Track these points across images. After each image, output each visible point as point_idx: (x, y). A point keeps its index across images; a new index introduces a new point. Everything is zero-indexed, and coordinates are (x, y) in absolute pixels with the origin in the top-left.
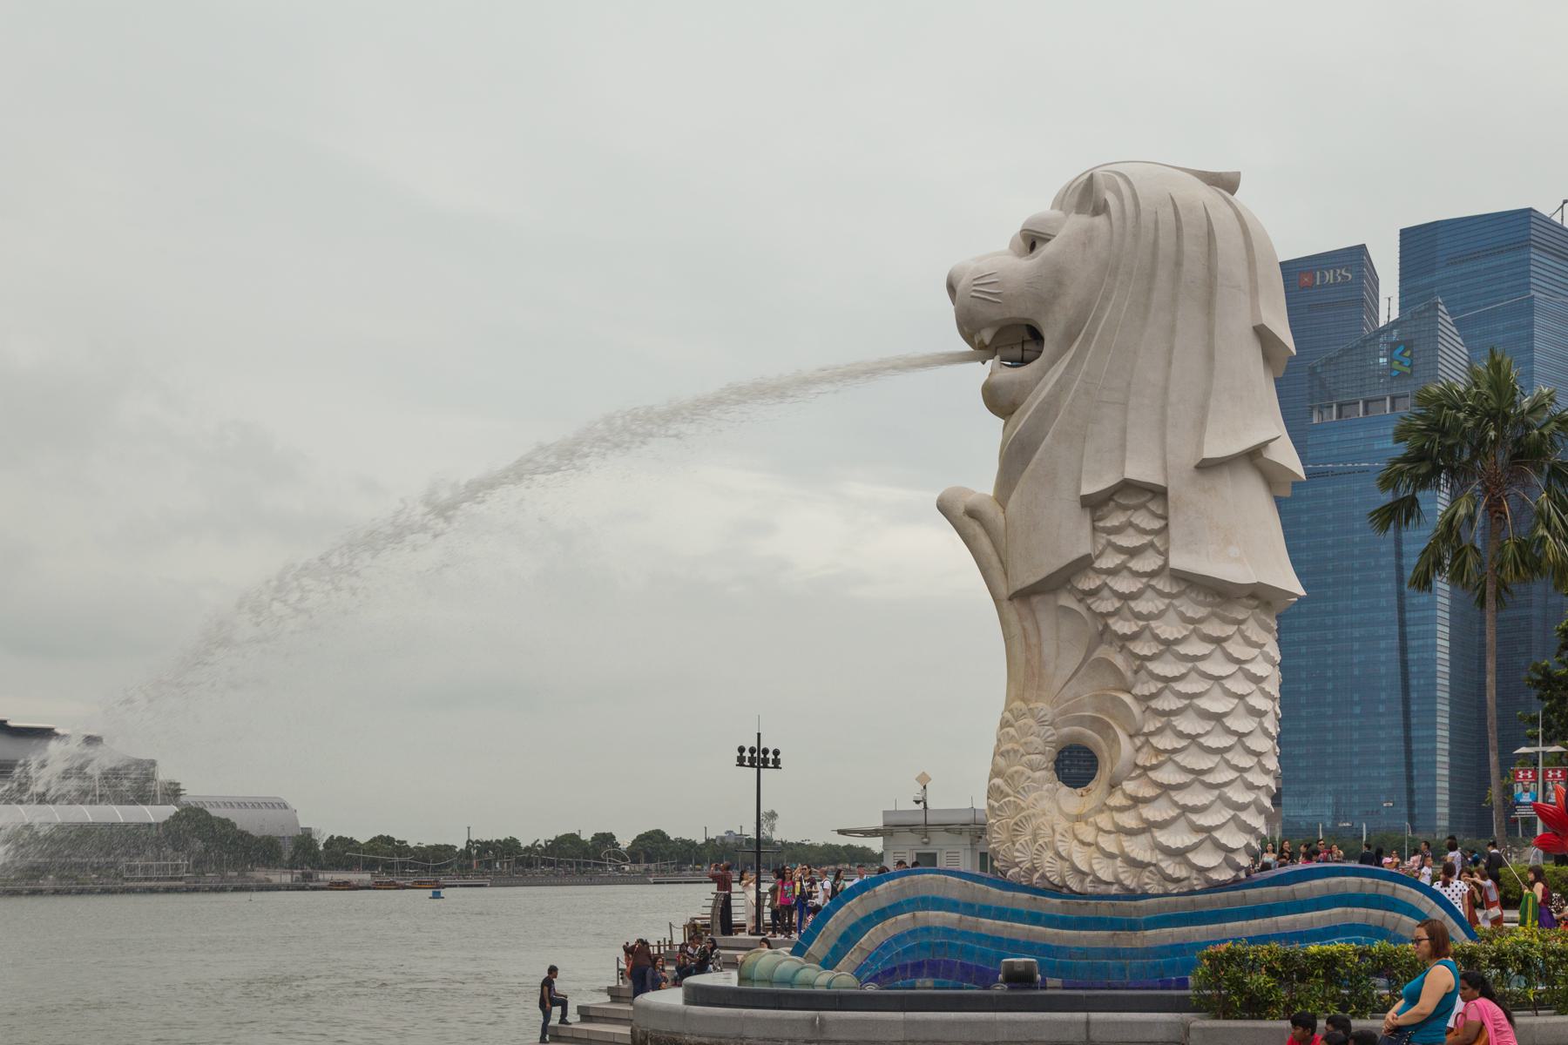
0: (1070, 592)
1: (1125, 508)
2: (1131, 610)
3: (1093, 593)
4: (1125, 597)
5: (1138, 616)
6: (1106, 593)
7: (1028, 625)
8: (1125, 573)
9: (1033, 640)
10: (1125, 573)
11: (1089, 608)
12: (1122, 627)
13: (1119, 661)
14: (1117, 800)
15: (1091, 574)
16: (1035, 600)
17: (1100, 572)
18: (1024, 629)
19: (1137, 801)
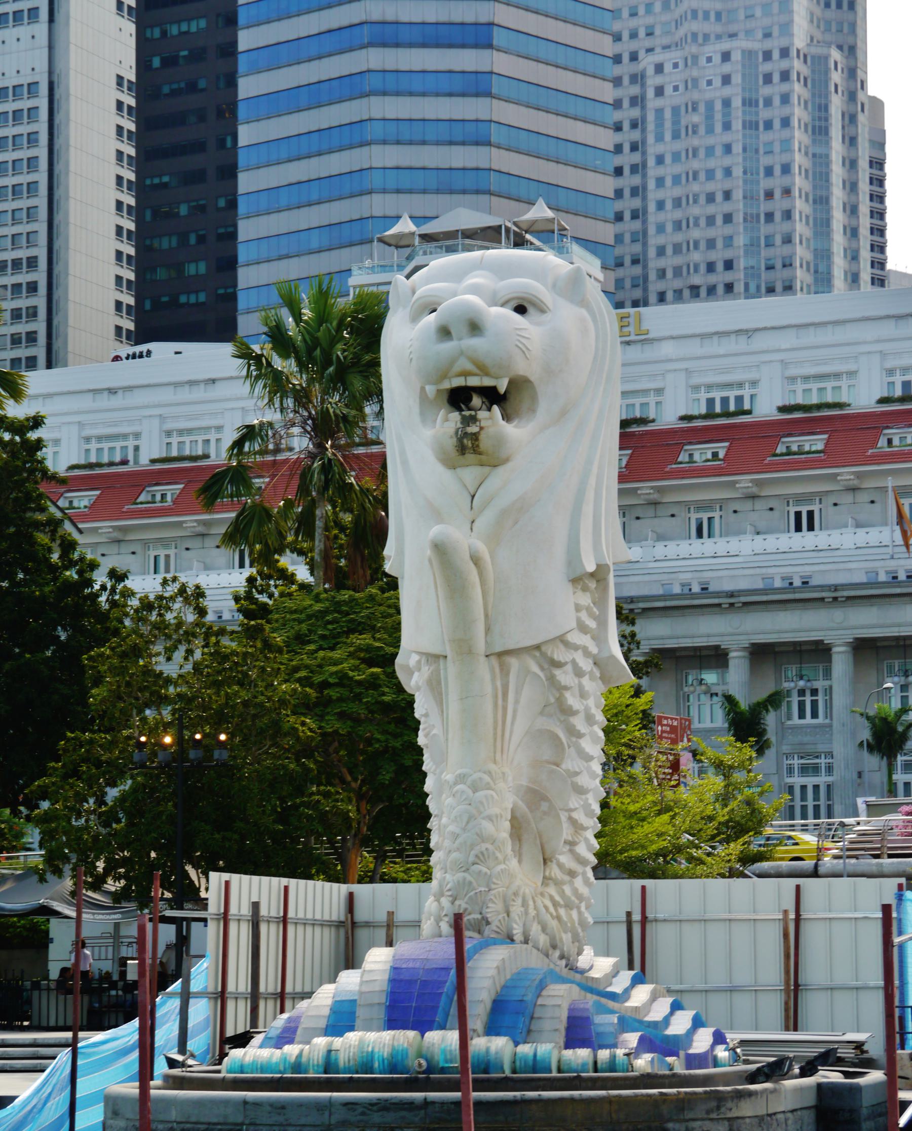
0: (534, 657)
1: (585, 589)
2: (581, 687)
3: (558, 665)
4: (579, 673)
5: (583, 695)
6: (569, 668)
7: (499, 684)
8: (580, 652)
9: (500, 702)
10: (580, 652)
11: (552, 679)
12: (572, 700)
13: (562, 735)
14: (555, 872)
15: (561, 646)
16: (513, 662)
17: (567, 644)
18: (495, 689)
19: (572, 874)
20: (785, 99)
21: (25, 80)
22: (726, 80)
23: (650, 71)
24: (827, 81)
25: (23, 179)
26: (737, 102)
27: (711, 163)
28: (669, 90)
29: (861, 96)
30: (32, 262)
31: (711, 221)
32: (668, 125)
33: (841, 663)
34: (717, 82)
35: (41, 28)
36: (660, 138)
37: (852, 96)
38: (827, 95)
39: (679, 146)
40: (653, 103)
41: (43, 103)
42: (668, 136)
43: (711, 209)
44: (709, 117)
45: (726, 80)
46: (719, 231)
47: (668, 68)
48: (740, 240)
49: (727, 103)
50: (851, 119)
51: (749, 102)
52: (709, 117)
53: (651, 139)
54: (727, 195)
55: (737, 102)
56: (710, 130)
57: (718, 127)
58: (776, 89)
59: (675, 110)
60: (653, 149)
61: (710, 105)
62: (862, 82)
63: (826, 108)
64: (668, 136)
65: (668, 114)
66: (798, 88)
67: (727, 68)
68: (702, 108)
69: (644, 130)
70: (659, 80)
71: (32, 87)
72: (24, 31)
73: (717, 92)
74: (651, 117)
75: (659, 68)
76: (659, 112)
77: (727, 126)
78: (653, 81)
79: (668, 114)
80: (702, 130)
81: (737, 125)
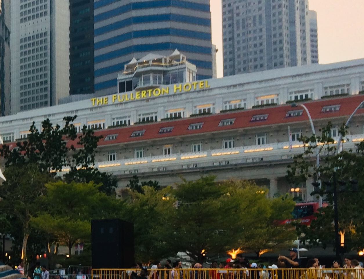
20: (280, 13)
21: (44, 31)
22: (260, 9)
23: (235, 8)
24: (294, 6)
25: (43, 59)
26: (264, 16)
27: (256, 35)
28: (241, 14)
29: (306, 10)
30: (46, 82)
31: (256, 53)
32: (241, 24)
33: (273, 185)
34: (257, 10)
35: (48, 17)
36: (238, 28)
37: (303, 10)
38: (294, 10)
39: (245, 31)
40: (236, 18)
41: (48, 37)
42: (241, 28)
43: (255, 49)
44: (255, 20)
45: (260, 9)
46: (258, 55)
47: (241, 7)
48: (266, 58)
49: (260, 16)
50: (303, 18)
51: (268, 16)
52: (255, 20)
53: (235, 29)
54: (261, 44)
55: (264, 16)
56: (255, 24)
57: (257, 23)
58: (277, 10)
59: (243, 20)
60: (236, 32)
61: (255, 17)
62: (307, 6)
63: (294, 14)
64: (241, 28)
65: (241, 22)
66: (284, 9)
67: (260, 5)
68: (252, 18)
69: (233, 27)
70: (238, 11)
71: (46, 33)
72: (43, 18)
73: (257, 13)
74: (235, 23)
75: (238, 8)
76: (238, 22)
77: (260, 23)
78: (236, 11)
79: (241, 22)
80: (252, 25)
81: (264, 22)
